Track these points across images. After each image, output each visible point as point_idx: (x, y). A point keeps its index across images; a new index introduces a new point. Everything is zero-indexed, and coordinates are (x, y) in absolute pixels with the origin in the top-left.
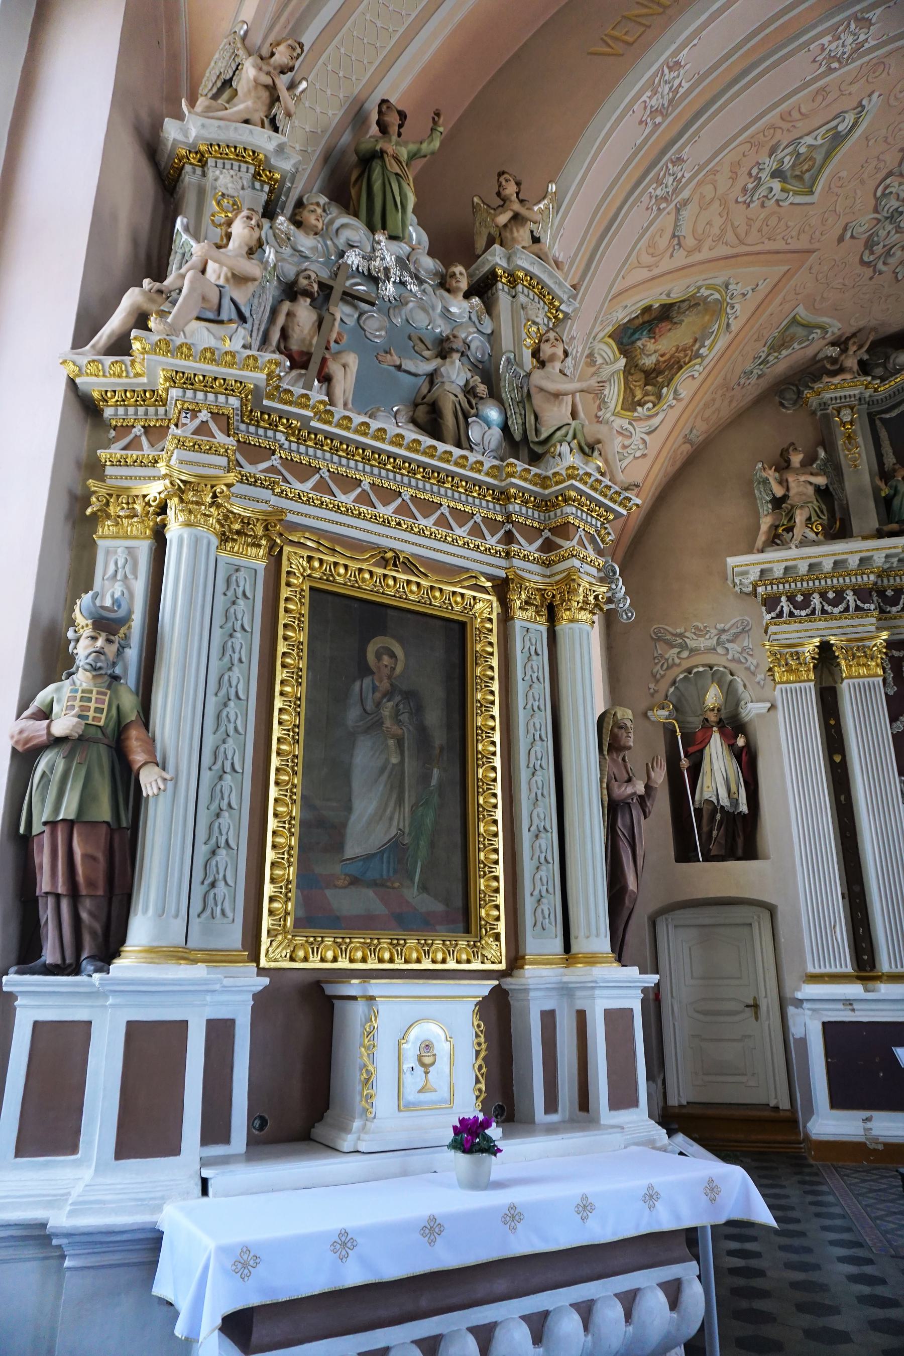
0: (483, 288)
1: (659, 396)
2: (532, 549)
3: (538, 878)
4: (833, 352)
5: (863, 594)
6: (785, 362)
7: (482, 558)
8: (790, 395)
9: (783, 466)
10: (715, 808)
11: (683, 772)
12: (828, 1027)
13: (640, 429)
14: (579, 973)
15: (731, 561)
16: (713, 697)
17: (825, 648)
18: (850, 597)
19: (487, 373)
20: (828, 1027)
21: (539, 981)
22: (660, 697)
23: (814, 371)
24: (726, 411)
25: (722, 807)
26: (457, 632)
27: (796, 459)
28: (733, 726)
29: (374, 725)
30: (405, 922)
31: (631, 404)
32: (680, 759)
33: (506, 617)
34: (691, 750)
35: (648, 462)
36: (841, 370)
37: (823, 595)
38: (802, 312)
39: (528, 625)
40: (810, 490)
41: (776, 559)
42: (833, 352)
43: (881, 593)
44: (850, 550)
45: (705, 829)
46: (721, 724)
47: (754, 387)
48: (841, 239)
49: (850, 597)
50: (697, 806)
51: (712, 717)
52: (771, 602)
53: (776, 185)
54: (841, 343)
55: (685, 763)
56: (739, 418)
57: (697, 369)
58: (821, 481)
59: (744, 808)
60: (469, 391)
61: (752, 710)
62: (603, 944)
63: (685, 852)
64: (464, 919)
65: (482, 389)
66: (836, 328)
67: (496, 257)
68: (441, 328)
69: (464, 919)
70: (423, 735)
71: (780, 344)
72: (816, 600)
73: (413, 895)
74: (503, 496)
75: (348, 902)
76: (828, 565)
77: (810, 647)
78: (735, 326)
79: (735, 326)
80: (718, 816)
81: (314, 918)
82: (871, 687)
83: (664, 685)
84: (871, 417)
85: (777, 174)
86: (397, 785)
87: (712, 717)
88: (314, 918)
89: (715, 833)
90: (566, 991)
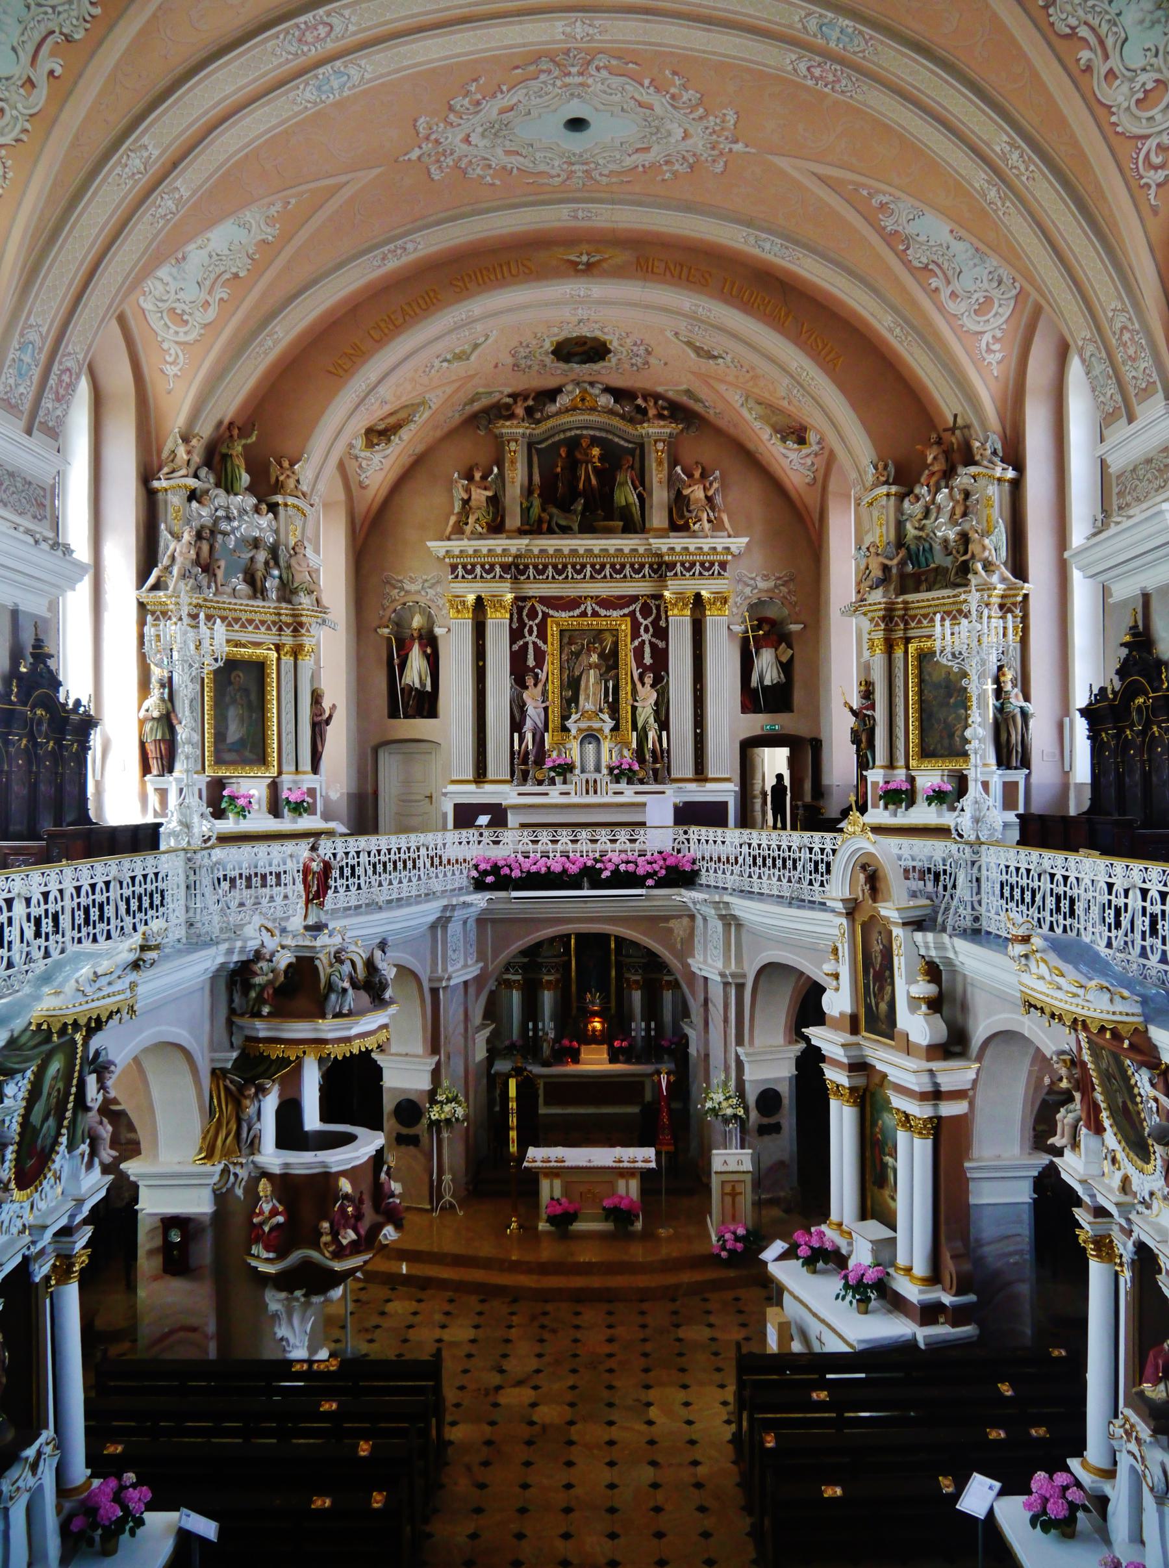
0: (273, 508)
1: (389, 440)
2: (288, 631)
3: (289, 748)
4: (509, 400)
5: (506, 568)
6: (477, 406)
7: (270, 638)
8: (484, 422)
9: (470, 477)
11: (395, 666)
12: (456, 805)
13: (377, 458)
14: (300, 777)
15: (429, 544)
16: (417, 622)
17: (479, 599)
18: (498, 569)
19: (274, 551)
20: (456, 805)
21: (287, 780)
22: (385, 620)
23: (499, 411)
24: (439, 434)
26: (260, 667)
27: (478, 476)
28: (430, 641)
29: (234, 701)
30: (244, 762)
31: (370, 445)
33: (279, 659)
35: (383, 474)
36: (512, 416)
37: (483, 566)
38: (481, 390)
39: (287, 660)
40: (484, 499)
41: (456, 546)
42: (509, 400)
43: (517, 566)
44: (498, 544)
46: (420, 637)
47: (457, 419)
48: (496, 366)
49: (498, 569)
51: (415, 634)
52: (454, 568)
53: (445, 364)
54: (514, 396)
56: (451, 434)
57: (412, 426)
58: (490, 493)
59: (429, 688)
60: (267, 563)
61: (439, 631)
62: (309, 768)
63: (393, 714)
64: (263, 760)
65: (272, 563)
66: (508, 390)
67: (279, 499)
68: (257, 534)
69: (263, 760)
70: (250, 702)
71: (472, 401)
72: (478, 569)
73: (247, 754)
74: (279, 614)
75: (228, 756)
76: (485, 551)
77: (471, 598)
78: (434, 407)
79: (434, 407)
81: (219, 761)
82: (502, 625)
83: (388, 612)
84: (530, 446)
85: (445, 360)
86: (242, 720)
87: (415, 634)
88: (219, 761)
90: (295, 782)
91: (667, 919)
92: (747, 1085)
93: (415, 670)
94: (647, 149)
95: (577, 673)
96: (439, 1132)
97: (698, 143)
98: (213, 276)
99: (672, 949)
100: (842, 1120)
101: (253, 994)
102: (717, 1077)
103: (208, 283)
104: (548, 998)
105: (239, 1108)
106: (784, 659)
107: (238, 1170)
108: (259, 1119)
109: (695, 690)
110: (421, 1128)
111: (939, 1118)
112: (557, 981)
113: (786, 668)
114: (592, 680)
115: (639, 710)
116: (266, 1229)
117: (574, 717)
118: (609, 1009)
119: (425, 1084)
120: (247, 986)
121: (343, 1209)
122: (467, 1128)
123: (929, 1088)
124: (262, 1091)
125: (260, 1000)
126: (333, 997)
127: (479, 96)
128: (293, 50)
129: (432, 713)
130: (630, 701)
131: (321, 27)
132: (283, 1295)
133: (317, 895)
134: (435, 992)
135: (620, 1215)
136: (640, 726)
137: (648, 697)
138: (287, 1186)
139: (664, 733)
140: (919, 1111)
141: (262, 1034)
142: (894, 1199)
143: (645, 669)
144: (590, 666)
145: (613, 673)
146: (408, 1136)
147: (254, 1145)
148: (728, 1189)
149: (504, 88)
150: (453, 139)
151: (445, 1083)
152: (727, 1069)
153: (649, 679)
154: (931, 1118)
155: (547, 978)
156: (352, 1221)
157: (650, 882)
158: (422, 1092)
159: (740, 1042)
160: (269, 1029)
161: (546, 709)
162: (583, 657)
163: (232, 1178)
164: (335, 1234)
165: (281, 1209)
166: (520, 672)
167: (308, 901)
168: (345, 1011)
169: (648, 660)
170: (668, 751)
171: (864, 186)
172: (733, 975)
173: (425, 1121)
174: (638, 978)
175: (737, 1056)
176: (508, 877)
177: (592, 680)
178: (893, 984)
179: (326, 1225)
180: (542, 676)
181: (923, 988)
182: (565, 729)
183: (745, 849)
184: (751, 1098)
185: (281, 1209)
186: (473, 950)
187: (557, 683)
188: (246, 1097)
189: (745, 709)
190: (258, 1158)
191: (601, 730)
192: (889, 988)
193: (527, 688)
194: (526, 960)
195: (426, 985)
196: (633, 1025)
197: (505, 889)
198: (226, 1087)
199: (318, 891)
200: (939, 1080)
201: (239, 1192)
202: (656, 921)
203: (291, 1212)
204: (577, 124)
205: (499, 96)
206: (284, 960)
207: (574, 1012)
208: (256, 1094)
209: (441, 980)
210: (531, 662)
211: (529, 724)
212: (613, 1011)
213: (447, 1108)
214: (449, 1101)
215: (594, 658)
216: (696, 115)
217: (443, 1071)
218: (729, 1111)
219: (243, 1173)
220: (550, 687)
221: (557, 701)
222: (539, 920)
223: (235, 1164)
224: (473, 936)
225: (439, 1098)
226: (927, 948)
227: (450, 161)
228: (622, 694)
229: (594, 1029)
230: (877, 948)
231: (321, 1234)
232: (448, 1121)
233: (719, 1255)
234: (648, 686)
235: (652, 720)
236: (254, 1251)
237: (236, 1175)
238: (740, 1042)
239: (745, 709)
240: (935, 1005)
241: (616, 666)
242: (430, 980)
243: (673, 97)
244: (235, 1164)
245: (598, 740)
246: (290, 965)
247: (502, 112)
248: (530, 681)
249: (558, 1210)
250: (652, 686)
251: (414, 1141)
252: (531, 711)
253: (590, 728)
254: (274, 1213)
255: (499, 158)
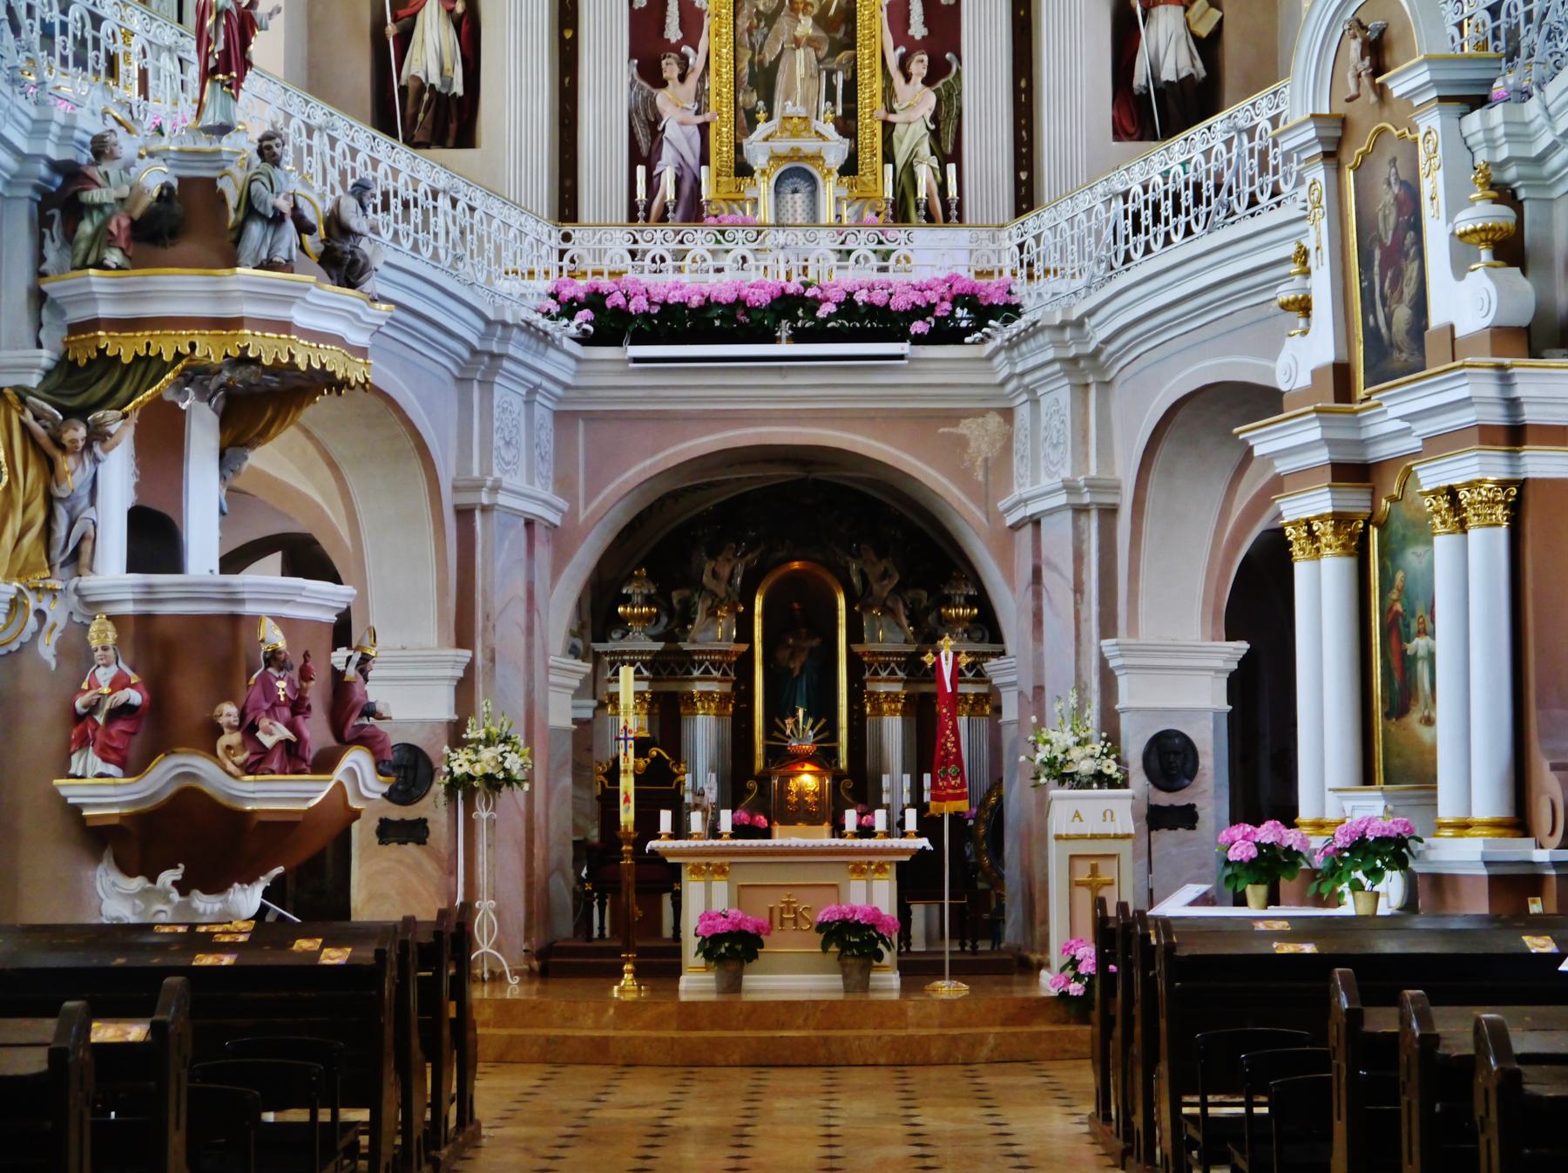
10: (422, 88)
25: (432, 86)
32: (386, 24)
34: (401, 13)
45: (410, 111)
50: (403, 83)
55: (391, 29)
59: (458, 89)
80: (426, 96)
89: (421, 116)
91: (953, 417)
92: (1126, 725)
93: (431, 53)
95: (769, 57)
96: (470, 808)
99: (962, 476)
100: (1320, 592)
101: (86, 228)
102: (1060, 704)
104: (704, 733)
105: (50, 468)
106: (1204, 30)
107: (46, 604)
108: (93, 502)
109: (1018, 183)
110: (433, 807)
111: (1522, 484)
112: (724, 698)
113: (1208, 47)
114: (800, 71)
115: (899, 129)
116: (100, 719)
117: (763, 128)
118: (833, 754)
119: (442, 708)
120: (74, 210)
121: (267, 686)
122: (530, 796)
123: (1496, 416)
124: (98, 435)
125: (103, 237)
126: (255, 230)
129: (466, 138)
130: (881, 112)
132: (138, 883)
133: (224, 65)
134: (464, 515)
135: (851, 940)
136: (900, 160)
137: (917, 103)
138: (148, 638)
139: (951, 168)
140: (1476, 468)
141: (105, 311)
142: (1429, 721)
143: (912, 47)
144: (797, 42)
145: (844, 56)
146: (403, 823)
147: (78, 558)
148: (1083, 873)
151: (483, 705)
152: (1080, 687)
153: (919, 66)
154: (1504, 484)
155: (698, 688)
156: (286, 713)
157: (918, 327)
158: (433, 724)
159: (1108, 627)
160: (121, 298)
161: (704, 128)
162: (784, 22)
163: (32, 622)
164: (249, 729)
165: (134, 679)
166: (649, 54)
167: (207, 74)
168: (281, 256)
169: (918, 30)
170: (960, 206)
172: (1093, 486)
173: (439, 786)
174: (897, 688)
175: (1103, 661)
176: (621, 313)
177: (800, 71)
178: (1420, 255)
179: (228, 712)
180: (696, 61)
181: (1482, 213)
182: (743, 170)
183: (1118, 205)
184: (1134, 749)
185: (134, 679)
186: (547, 468)
187: (727, 73)
188: (63, 448)
189: (1120, 133)
190: (87, 581)
191: (817, 158)
192: (1412, 270)
193: (663, 84)
194: (659, 646)
195: (448, 501)
196: (886, 779)
197: (617, 342)
198: (25, 427)
199: (225, 54)
200: (1520, 391)
201: (47, 649)
202: (933, 422)
203: (157, 687)
206: (154, 178)
207: (759, 764)
208: (88, 446)
209: (477, 487)
210: (673, 33)
211: (667, 153)
212: (843, 764)
213: (487, 754)
214: (488, 742)
215: (806, 26)
217: (480, 687)
218: (1086, 767)
219: (57, 613)
220: (712, 83)
221: (728, 112)
222: (687, 417)
223: (37, 590)
224: (547, 435)
225: (471, 734)
226: (1491, 144)
228: (863, 96)
229: (801, 793)
230: (1386, 196)
231: (218, 731)
232: (488, 778)
233: (1064, 995)
234: (917, 80)
235: (925, 149)
236: (76, 766)
237: (40, 614)
238: (1108, 627)
239: (1120, 133)
240: (1510, 249)
241: (850, 43)
242: (456, 489)
244: (37, 590)
245: (812, 180)
246: (166, 187)
248: (670, 69)
249: (722, 927)
250: (928, 81)
251: (415, 832)
252: (672, 130)
253: (796, 155)
254: (119, 683)
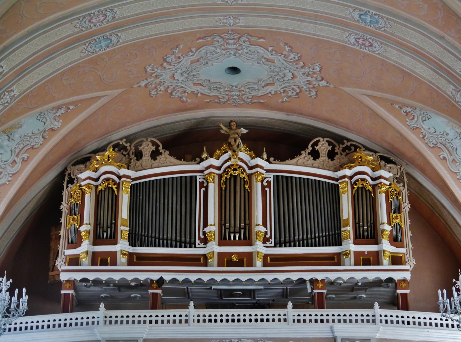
94: (273, 84)
97: (301, 80)
98: (21, 146)
103: (17, 151)
127: (180, 55)
128: (85, 26)
131: (101, 16)
149: (194, 50)
150: (166, 76)
171: (397, 103)
204: (234, 70)
205: (191, 54)
216: (299, 66)
227: (162, 88)
243: (285, 56)
247: (192, 62)
255: (191, 88)
